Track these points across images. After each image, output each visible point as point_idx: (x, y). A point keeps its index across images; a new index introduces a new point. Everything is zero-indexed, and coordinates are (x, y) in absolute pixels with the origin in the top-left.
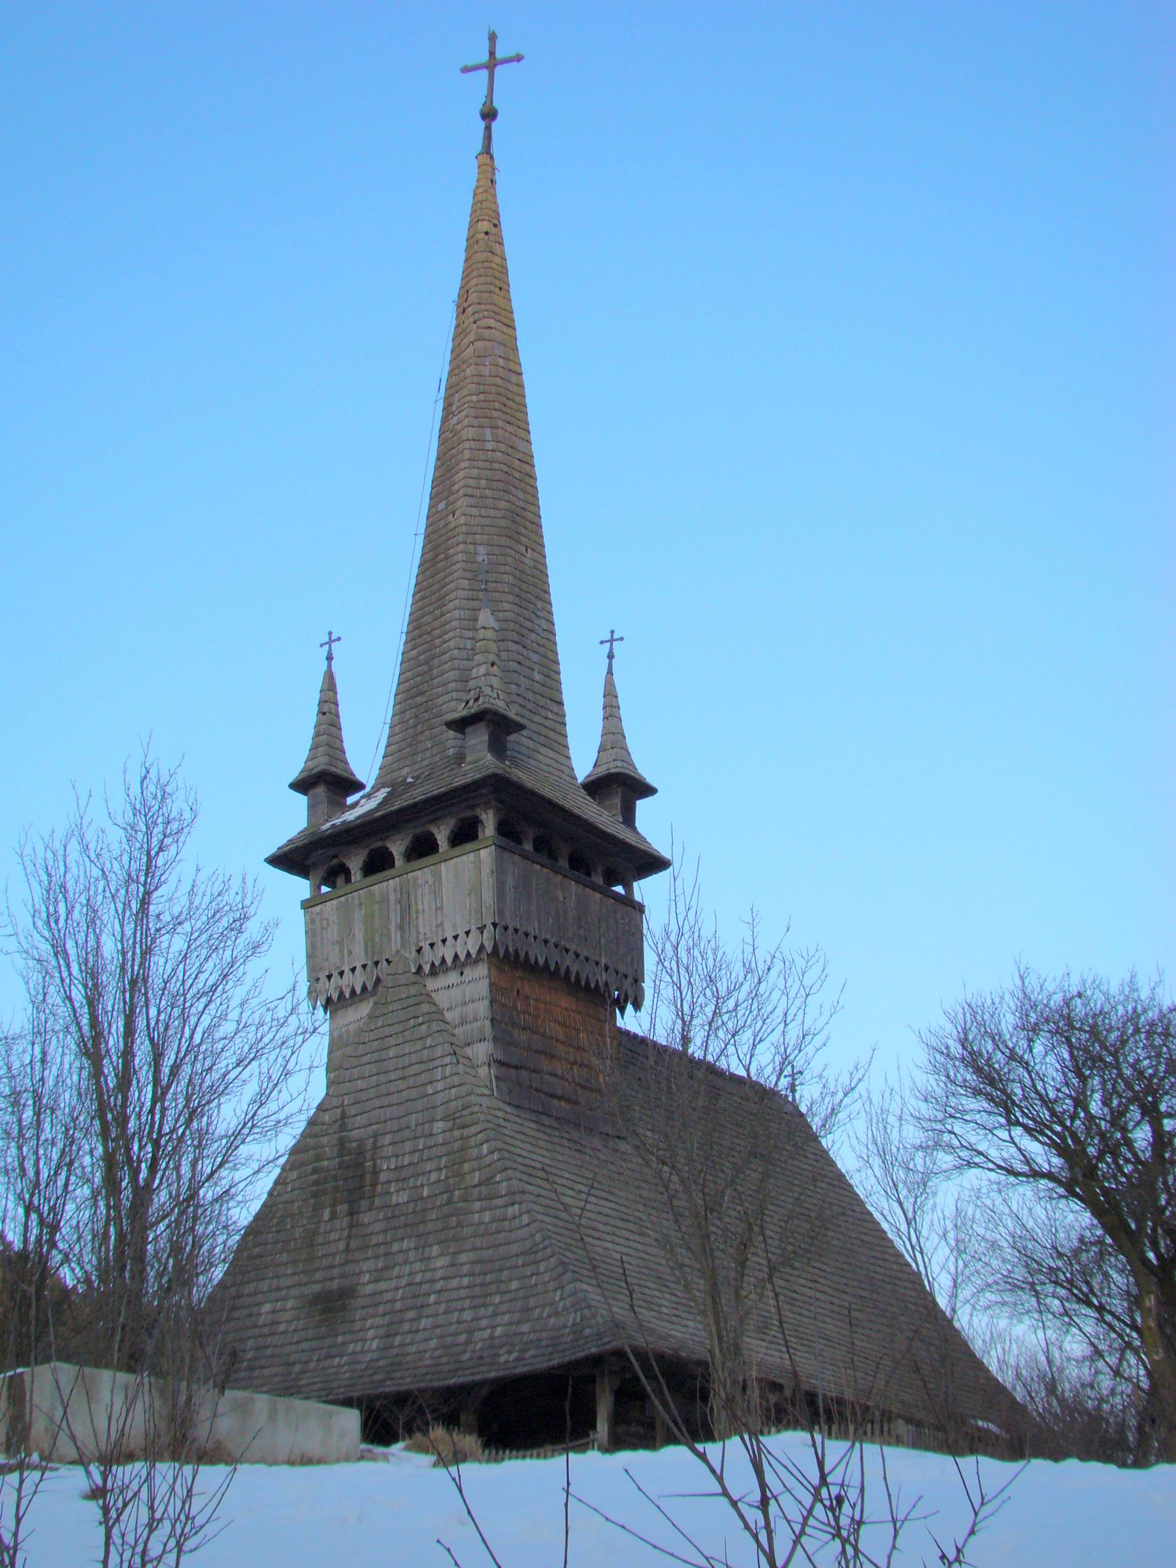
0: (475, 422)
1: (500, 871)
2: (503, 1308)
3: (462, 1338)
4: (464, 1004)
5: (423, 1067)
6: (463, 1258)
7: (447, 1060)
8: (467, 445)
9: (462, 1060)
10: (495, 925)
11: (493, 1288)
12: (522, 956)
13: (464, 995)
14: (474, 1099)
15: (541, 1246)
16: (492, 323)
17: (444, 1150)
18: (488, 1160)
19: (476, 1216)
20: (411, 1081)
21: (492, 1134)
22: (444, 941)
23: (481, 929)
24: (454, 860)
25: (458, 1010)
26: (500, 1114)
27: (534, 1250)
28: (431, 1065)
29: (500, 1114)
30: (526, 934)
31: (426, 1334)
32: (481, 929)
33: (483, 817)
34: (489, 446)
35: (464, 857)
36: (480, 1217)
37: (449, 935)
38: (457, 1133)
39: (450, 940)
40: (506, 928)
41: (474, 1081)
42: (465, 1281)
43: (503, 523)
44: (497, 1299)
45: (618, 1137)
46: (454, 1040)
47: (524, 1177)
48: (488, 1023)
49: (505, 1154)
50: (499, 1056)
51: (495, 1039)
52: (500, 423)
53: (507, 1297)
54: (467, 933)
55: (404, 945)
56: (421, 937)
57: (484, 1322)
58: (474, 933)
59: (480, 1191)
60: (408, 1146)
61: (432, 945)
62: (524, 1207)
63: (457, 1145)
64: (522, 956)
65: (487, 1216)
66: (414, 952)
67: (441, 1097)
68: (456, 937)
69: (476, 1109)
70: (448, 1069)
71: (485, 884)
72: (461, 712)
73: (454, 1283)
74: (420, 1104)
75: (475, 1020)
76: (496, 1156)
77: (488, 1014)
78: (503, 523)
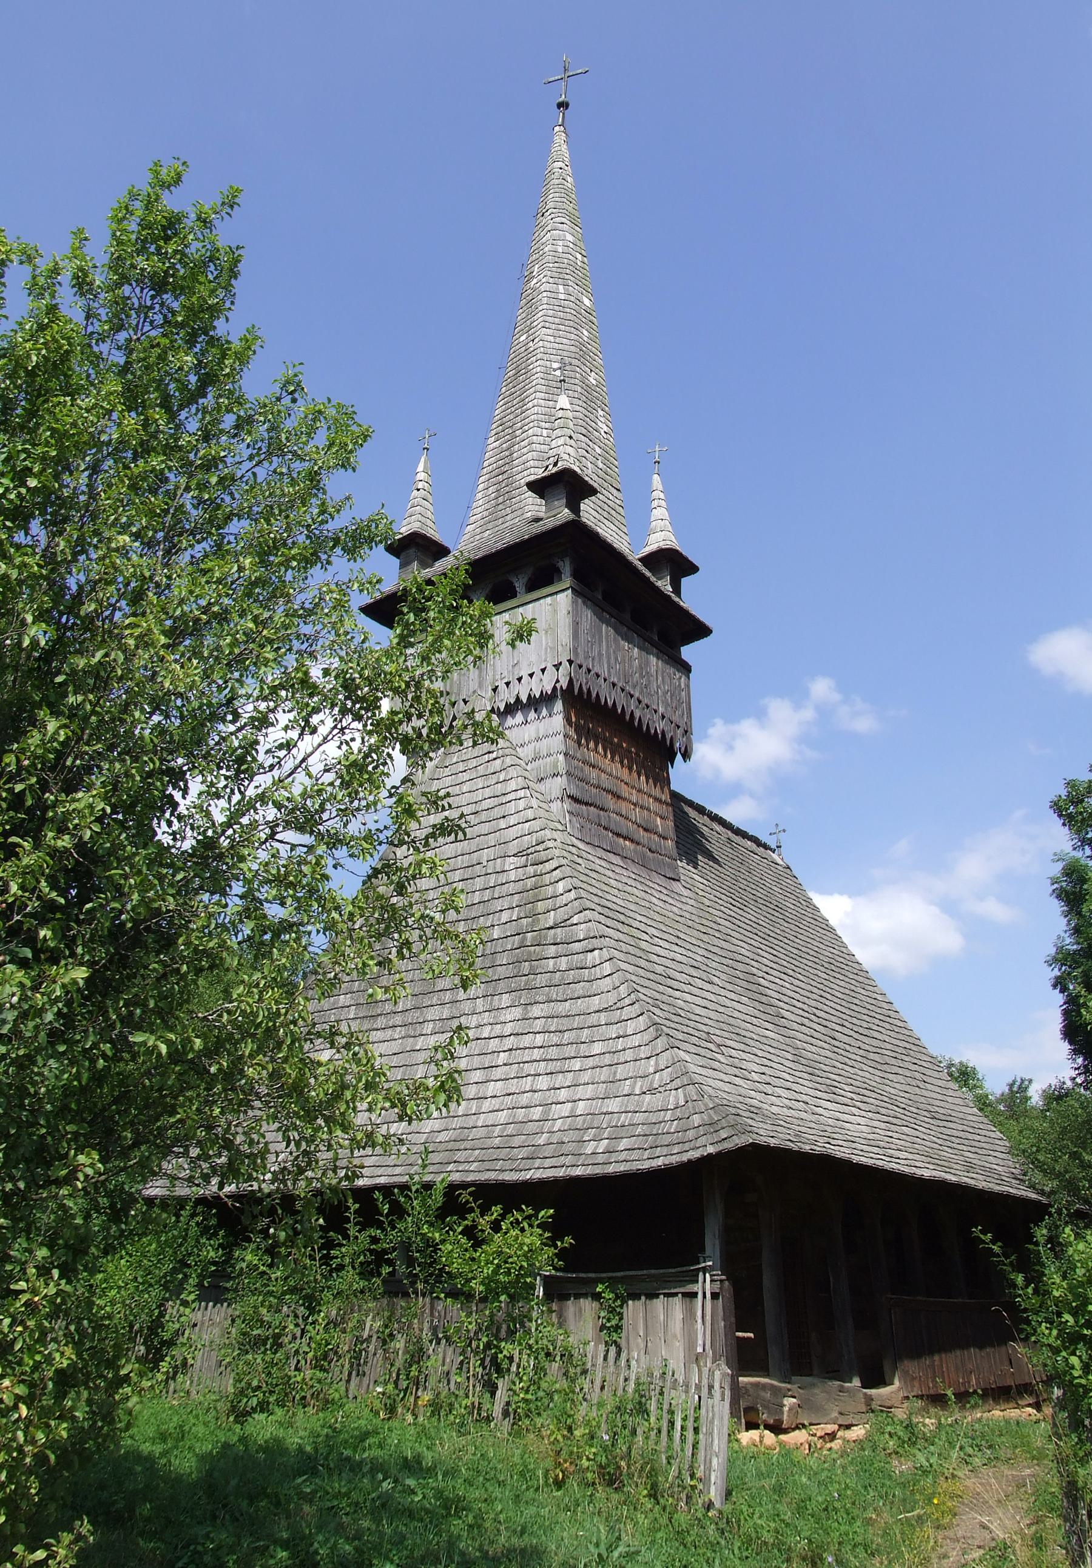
0: (551, 280)
1: (575, 614)
2: (586, 1077)
3: (537, 1113)
4: (538, 739)
5: (496, 801)
6: (536, 1011)
7: (521, 793)
8: (545, 294)
9: (535, 794)
10: (570, 662)
11: (570, 1051)
12: (594, 695)
13: (538, 730)
14: (548, 833)
15: (627, 1001)
16: (564, 220)
17: (519, 886)
18: (564, 899)
19: (551, 962)
20: (483, 816)
21: (567, 871)
22: (520, 679)
23: (557, 667)
24: (530, 605)
25: (531, 746)
26: (574, 850)
27: (619, 1005)
28: (504, 799)
29: (574, 850)
30: (598, 676)
31: (495, 1103)
32: (557, 667)
33: (561, 564)
34: (562, 296)
35: (542, 601)
36: (555, 964)
37: (524, 673)
38: (531, 870)
39: (526, 678)
40: (580, 666)
41: (547, 815)
42: (539, 1039)
43: (573, 349)
44: (577, 1064)
45: (674, 879)
46: (526, 774)
47: (602, 919)
48: (561, 757)
49: (583, 894)
50: (573, 791)
51: (568, 774)
52: (571, 283)
53: (590, 1062)
54: (543, 670)
55: (480, 686)
56: (498, 677)
57: (563, 1094)
58: (550, 670)
59: (555, 934)
60: (479, 883)
61: (508, 684)
62: (606, 954)
63: (530, 883)
64: (594, 695)
65: (563, 963)
66: (490, 692)
67: (513, 833)
68: (531, 675)
69: (550, 844)
70: (522, 804)
71: (561, 623)
72: (540, 473)
73: (527, 1040)
74: (492, 839)
75: (549, 755)
76: (572, 895)
77: (563, 748)
78: (573, 349)
